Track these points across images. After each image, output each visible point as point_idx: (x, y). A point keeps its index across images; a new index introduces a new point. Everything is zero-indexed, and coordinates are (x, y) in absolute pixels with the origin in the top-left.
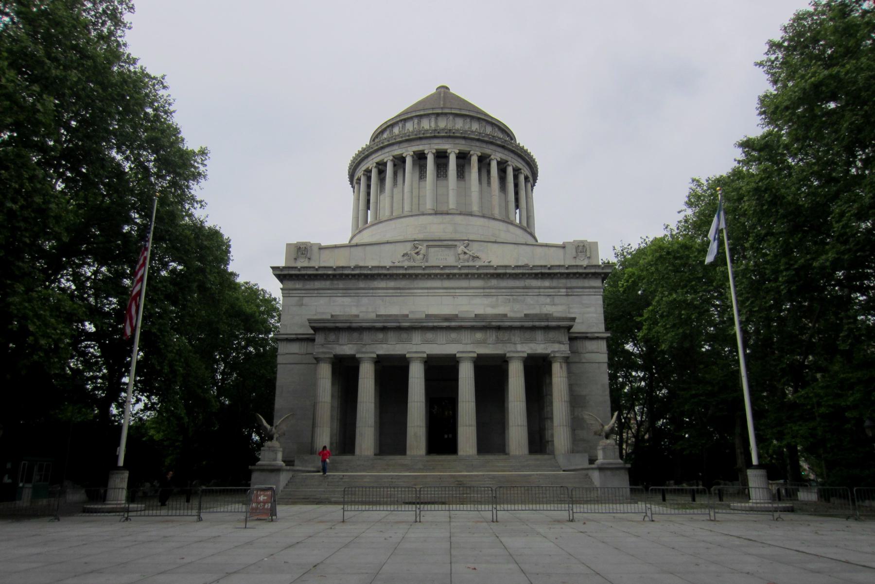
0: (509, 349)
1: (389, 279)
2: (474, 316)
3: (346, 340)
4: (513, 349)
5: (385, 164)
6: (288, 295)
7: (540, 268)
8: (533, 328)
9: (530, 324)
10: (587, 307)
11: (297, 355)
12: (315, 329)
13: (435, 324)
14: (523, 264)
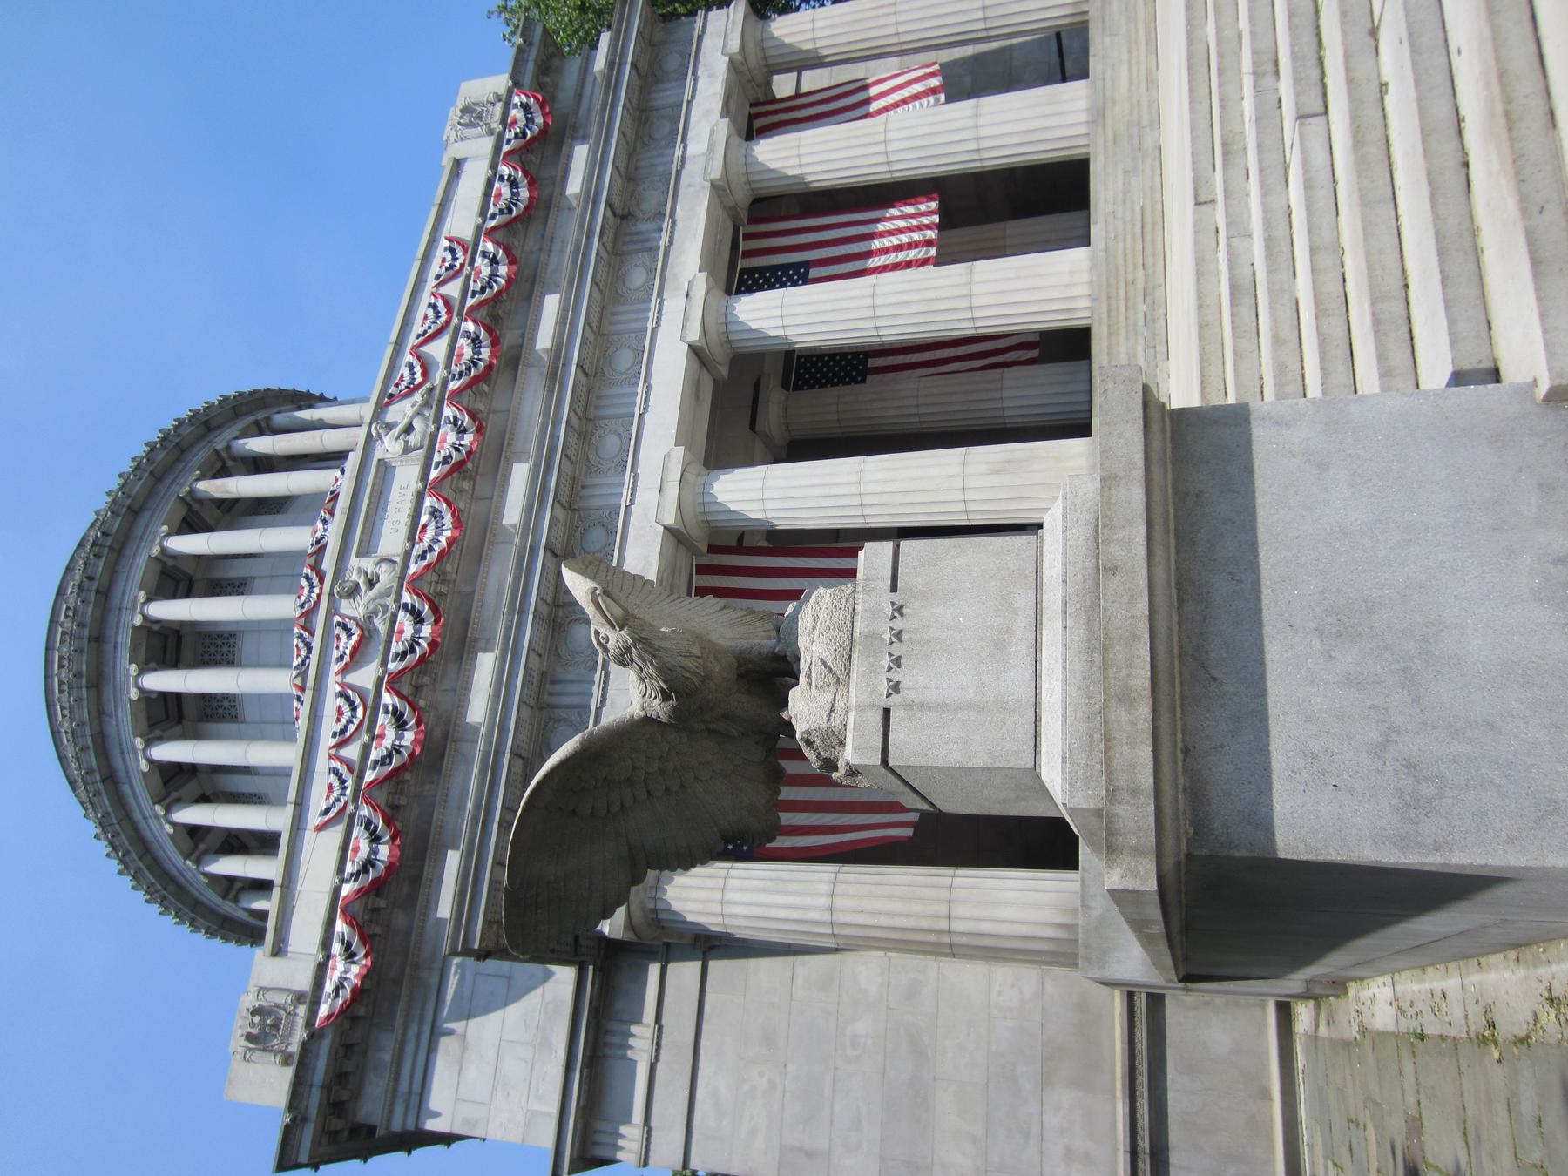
0: (699, 179)
6: (415, 1100)
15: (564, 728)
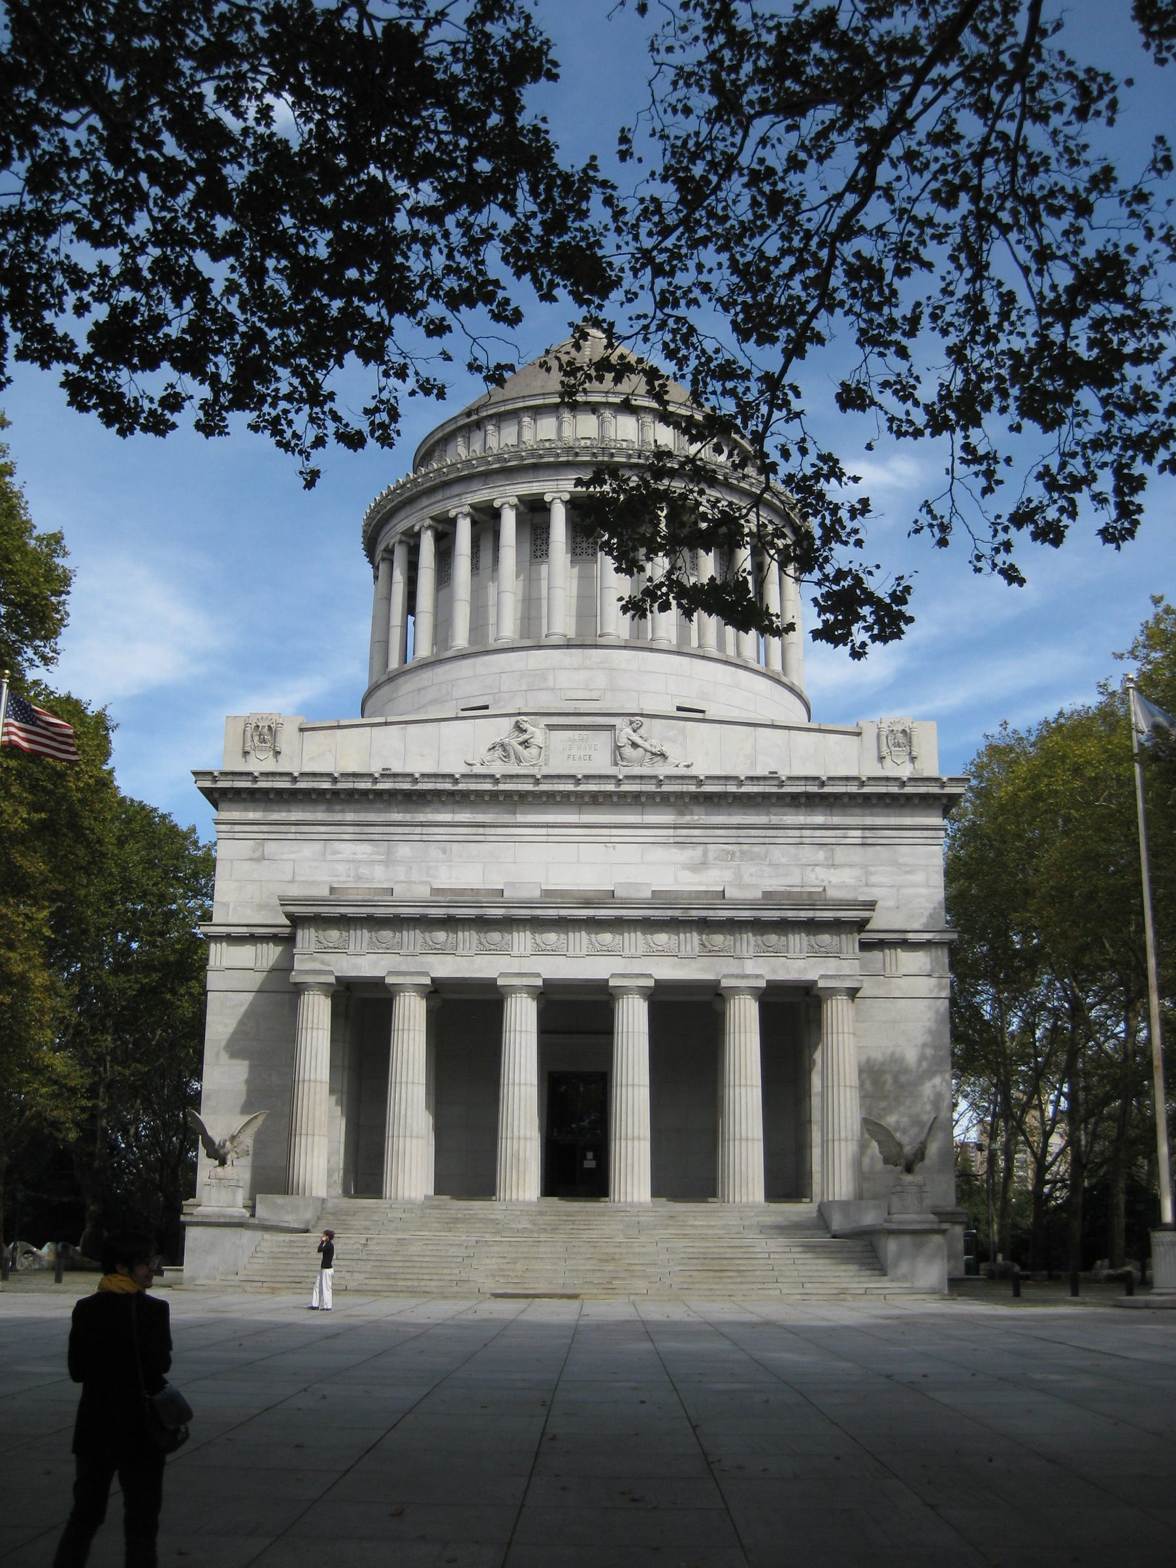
0: (726, 971)
1: (458, 802)
2: (649, 895)
4: (735, 972)
5: (453, 522)
7: (803, 783)
8: (784, 926)
9: (775, 915)
10: (907, 872)
12: (297, 921)
13: (563, 912)
14: (766, 773)
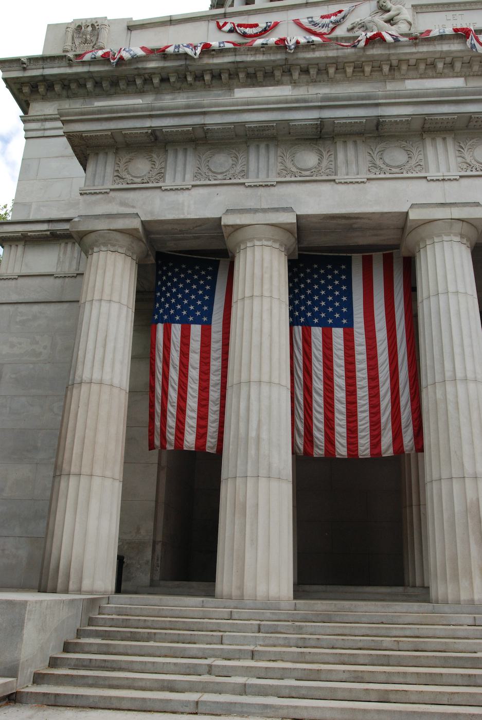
3: (189, 176)
11: (51, 280)
15: (231, 162)
